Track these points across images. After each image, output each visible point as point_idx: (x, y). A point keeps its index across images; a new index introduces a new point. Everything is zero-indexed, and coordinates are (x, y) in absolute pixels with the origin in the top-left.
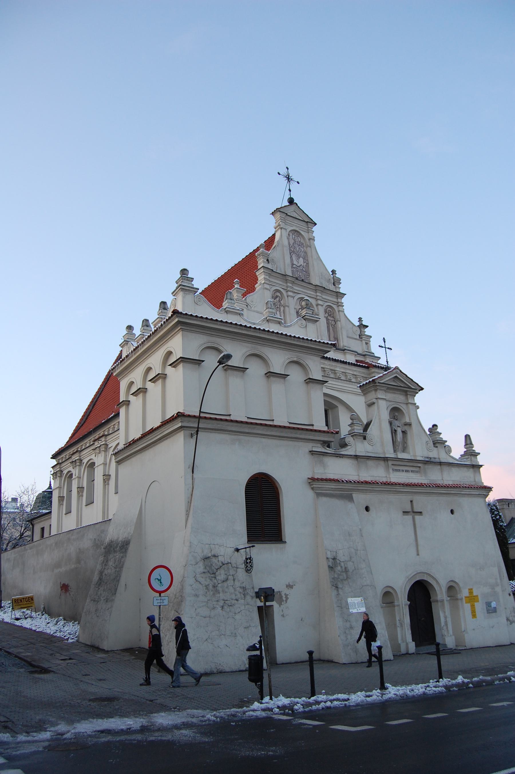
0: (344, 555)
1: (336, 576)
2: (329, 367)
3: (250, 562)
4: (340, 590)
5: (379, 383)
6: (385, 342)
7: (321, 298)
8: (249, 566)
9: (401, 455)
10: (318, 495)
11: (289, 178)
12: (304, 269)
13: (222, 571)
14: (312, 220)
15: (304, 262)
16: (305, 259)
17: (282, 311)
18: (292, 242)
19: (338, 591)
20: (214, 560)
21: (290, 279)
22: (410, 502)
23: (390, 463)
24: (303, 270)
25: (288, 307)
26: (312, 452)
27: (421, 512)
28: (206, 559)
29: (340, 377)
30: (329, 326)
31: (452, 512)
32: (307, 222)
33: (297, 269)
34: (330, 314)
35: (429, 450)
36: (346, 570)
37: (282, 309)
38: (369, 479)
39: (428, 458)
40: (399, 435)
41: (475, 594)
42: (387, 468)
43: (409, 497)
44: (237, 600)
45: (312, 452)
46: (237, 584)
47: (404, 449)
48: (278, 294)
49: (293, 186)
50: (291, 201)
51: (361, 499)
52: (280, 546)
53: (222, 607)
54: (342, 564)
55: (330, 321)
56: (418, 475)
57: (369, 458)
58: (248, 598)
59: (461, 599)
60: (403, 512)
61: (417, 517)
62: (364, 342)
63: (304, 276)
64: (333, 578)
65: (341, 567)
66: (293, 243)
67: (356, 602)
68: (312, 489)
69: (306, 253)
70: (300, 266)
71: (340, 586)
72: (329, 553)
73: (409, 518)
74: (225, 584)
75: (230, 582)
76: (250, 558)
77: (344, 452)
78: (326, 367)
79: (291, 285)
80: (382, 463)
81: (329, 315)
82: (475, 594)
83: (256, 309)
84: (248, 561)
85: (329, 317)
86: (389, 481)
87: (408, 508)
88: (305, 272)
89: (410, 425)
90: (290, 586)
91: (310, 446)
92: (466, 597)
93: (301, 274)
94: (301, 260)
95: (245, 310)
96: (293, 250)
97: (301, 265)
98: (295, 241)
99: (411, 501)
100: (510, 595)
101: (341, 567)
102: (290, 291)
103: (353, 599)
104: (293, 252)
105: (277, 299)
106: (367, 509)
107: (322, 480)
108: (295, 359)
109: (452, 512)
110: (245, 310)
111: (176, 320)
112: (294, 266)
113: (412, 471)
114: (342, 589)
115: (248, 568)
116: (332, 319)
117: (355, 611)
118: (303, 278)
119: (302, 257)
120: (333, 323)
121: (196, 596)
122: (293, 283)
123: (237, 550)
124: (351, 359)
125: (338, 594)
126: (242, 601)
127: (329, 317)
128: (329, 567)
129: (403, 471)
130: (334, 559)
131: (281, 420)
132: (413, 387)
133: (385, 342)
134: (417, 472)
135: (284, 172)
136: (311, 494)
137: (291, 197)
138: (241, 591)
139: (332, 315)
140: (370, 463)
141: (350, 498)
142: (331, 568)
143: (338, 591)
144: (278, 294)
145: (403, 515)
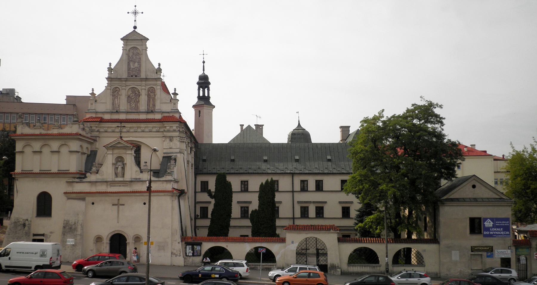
0: (72, 223)
1: (65, 230)
2: (136, 126)
4: (65, 236)
5: (107, 147)
7: (144, 85)
9: (117, 179)
10: (69, 199)
11: (135, 13)
12: (138, 69)
13: (20, 227)
14: (145, 37)
15: (138, 65)
16: (139, 63)
17: (119, 98)
18: (131, 54)
19: (64, 236)
20: (18, 223)
21: (123, 80)
22: (117, 200)
23: (109, 183)
24: (137, 70)
25: (121, 95)
26: (67, 182)
27: (124, 204)
28: (15, 222)
29: (143, 130)
30: (150, 99)
32: (141, 40)
33: (133, 70)
34: (152, 91)
36: (71, 228)
37: (119, 97)
38: (100, 191)
39: (135, 179)
40: (120, 169)
42: (107, 186)
43: (118, 198)
44: (23, 236)
45: (67, 182)
47: (123, 176)
48: (118, 89)
49: (139, 16)
50: (135, 27)
51: (89, 199)
52: (49, 218)
54: (70, 226)
55: (151, 96)
56: (127, 187)
57: (96, 182)
59: (142, 243)
60: (113, 204)
61: (120, 207)
62: (172, 104)
63: (137, 73)
64: (63, 231)
65: (69, 227)
66: (132, 56)
67: (71, 240)
68: (66, 196)
69: (140, 58)
70: (135, 68)
71: (66, 234)
73: (117, 207)
77: (84, 180)
78: (134, 126)
79: (124, 82)
80: (105, 183)
81: (151, 92)
83: (100, 102)
85: (151, 94)
86: (106, 191)
87: (116, 202)
88: (139, 70)
89: (126, 164)
90: (51, 233)
91: (67, 180)
92: (145, 242)
93: (135, 73)
94: (136, 64)
95: (94, 104)
96: (131, 59)
97: (136, 67)
98: (133, 53)
99: (119, 200)
100: (179, 243)
101: (69, 227)
102: (123, 86)
103: (70, 239)
104: (131, 61)
105: (117, 92)
106: (93, 204)
107: (70, 193)
108: (64, 143)
110: (94, 104)
112: (131, 69)
113: (123, 186)
114: (66, 235)
116: (153, 94)
117: (69, 244)
118: (136, 75)
119: (138, 62)
120: (154, 96)
121: (9, 234)
122: (126, 81)
124: (158, 117)
125: (64, 237)
127: (151, 94)
128: (63, 227)
129: (117, 186)
130: (67, 224)
131: (55, 170)
132: (129, 146)
134: (126, 186)
135: (132, 9)
136: (65, 198)
137: (136, 25)
138: (25, 233)
140: (98, 184)
141: (83, 199)
142: (64, 227)
144: (118, 89)
145: (113, 206)
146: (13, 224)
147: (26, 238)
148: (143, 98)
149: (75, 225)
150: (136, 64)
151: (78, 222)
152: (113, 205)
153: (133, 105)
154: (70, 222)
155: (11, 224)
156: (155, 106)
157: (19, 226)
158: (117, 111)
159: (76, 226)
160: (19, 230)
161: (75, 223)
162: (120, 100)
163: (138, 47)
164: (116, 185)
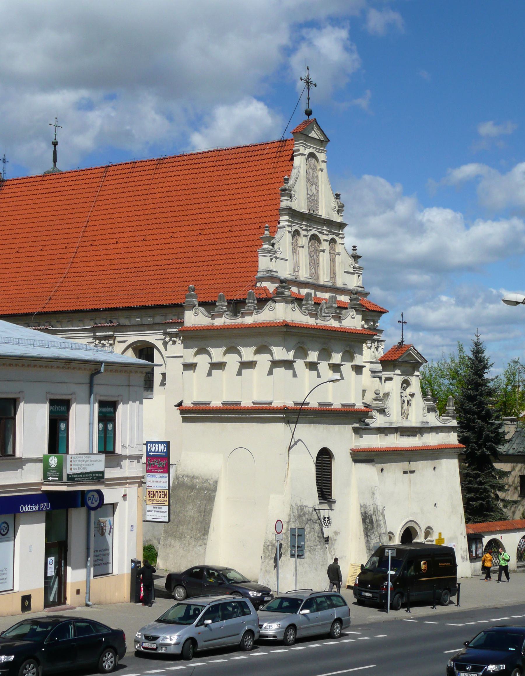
3: (328, 521)
6: (402, 316)
8: (327, 522)
16: (317, 185)
19: (367, 538)
31: (434, 468)
35: (424, 416)
41: (442, 537)
44: (316, 546)
46: (316, 534)
53: (310, 551)
58: (322, 544)
62: (356, 275)
69: (317, 177)
71: (369, 534)
72: (362, 508)
74: (310, 535)
75: (312, 533)
76: (328, 518)
82: (442, 537)
84: (327, 519)
100: (465, 537)
109: (434, 468)
111: (285, 330)
115: (325, 524)
123: (315, 510)
126: (319, 547)
132: (420, 361)
133: (402, 316)
139: (333, 248)
143: (367, 538)
145: (404, 473)
146: (298, 521)
147: (322, 548)
148: (324, 258)
149: (376, 515)
150: (314, 186)
151: (377, 509)
152: (405, 472)
153: (313, 269)
154: (368, 508)
155: (296, 520)
156: (336, 276)
157: (307, 523)
158: (296, 278)
159: (377, 516)
160: (309, 533)
161: (375, 512)
162: (299, 258)
163: (317, 154)
164: (405, 434)
